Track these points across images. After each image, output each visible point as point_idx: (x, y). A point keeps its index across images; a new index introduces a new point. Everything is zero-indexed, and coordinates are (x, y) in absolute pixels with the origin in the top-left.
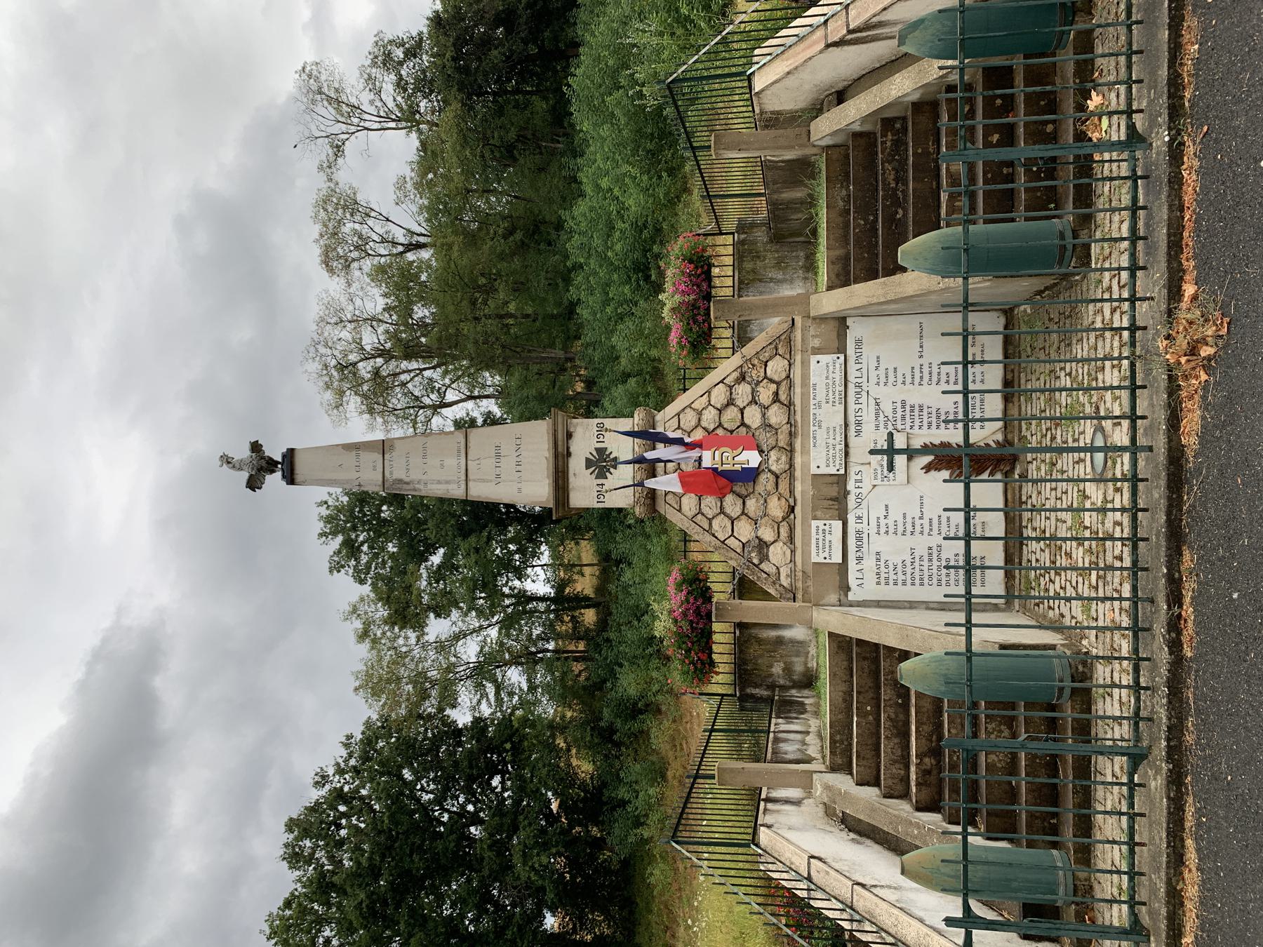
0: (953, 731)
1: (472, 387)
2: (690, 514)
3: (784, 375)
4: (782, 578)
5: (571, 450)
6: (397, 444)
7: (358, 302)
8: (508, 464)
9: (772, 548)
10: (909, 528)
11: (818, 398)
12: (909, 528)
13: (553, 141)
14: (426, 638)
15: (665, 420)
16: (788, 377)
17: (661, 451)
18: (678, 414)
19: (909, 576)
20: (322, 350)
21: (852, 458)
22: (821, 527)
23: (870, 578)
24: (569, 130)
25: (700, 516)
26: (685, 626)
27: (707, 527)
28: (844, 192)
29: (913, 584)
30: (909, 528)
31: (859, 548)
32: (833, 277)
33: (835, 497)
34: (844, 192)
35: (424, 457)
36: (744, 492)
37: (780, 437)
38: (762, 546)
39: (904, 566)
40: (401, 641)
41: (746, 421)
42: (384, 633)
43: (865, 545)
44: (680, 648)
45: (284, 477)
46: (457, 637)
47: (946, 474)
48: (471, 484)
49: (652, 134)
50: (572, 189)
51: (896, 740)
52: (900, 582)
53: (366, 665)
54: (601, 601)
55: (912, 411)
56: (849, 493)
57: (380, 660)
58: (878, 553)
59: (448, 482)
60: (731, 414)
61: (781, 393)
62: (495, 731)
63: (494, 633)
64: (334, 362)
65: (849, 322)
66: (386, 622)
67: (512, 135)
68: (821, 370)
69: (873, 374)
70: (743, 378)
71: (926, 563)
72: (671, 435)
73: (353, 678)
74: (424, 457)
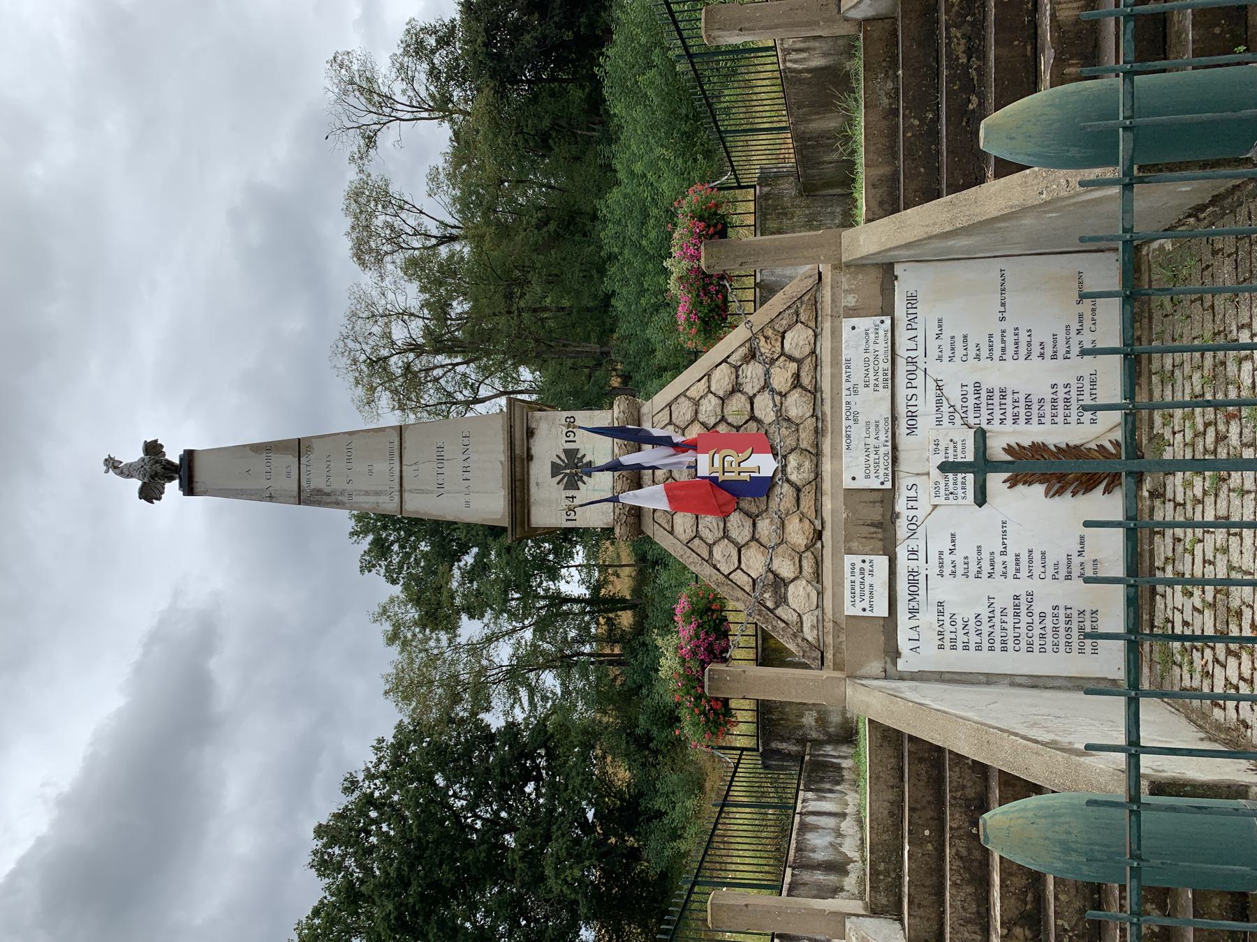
0: (1063, 897)
1: (504, 380)
3: (807, 350)
4: (806, 628)
5: (533, 452)
6: (316, 444)
7: (390, 296)
8: (453, 469)
9: (791, 588)
11: (853, 380)
13: (589, 129)
14: (458, 640)
16: (813, 352)
17: (647, 455)
18: (670, 405)
20: (351, 344)
21: (903, 466)
22: (859, 565)
23: (929, 640)
24: (604, 118)
25: (697, 541)
27: (706, 556)
28: (890, 85)
29: (991, 649)
30: (986, 568)
31: (913, 595)
32: (874, 204)
33: (878, 521)
34: (890, 85)
35: (349, 460)
36: (754, 510)
37: (803, 435)
38: (779, 584)
40: (432, 643)
41: (757, 413)
42: (414, 635)
43: (922, 592)
44: (688, 693)
45: (181, 486)
46: (489, 639)
48: (406, 495)
49: (687, 116)
50: (607, 176)
51: (970, 890)
52: (972, 646)
53: (396, 667)
54: (637, 604)
55: (990, 398)
56: (898, 516)
57: (412, 662)
58: (940, 604)
59: (377, 493)
60: (738, 404)
61: (803, 374)
62: (531, 736)
63: (528, 635)
64: (363, 357)
65: (898, 270)
66: (415, 624)
67: (546, 123)
68: (859, 338)
69: (933, 345)
70: (754, 357)
71: (1010, 619)
72: (657, 432)
73: (382, 681)
74: (349, 460)
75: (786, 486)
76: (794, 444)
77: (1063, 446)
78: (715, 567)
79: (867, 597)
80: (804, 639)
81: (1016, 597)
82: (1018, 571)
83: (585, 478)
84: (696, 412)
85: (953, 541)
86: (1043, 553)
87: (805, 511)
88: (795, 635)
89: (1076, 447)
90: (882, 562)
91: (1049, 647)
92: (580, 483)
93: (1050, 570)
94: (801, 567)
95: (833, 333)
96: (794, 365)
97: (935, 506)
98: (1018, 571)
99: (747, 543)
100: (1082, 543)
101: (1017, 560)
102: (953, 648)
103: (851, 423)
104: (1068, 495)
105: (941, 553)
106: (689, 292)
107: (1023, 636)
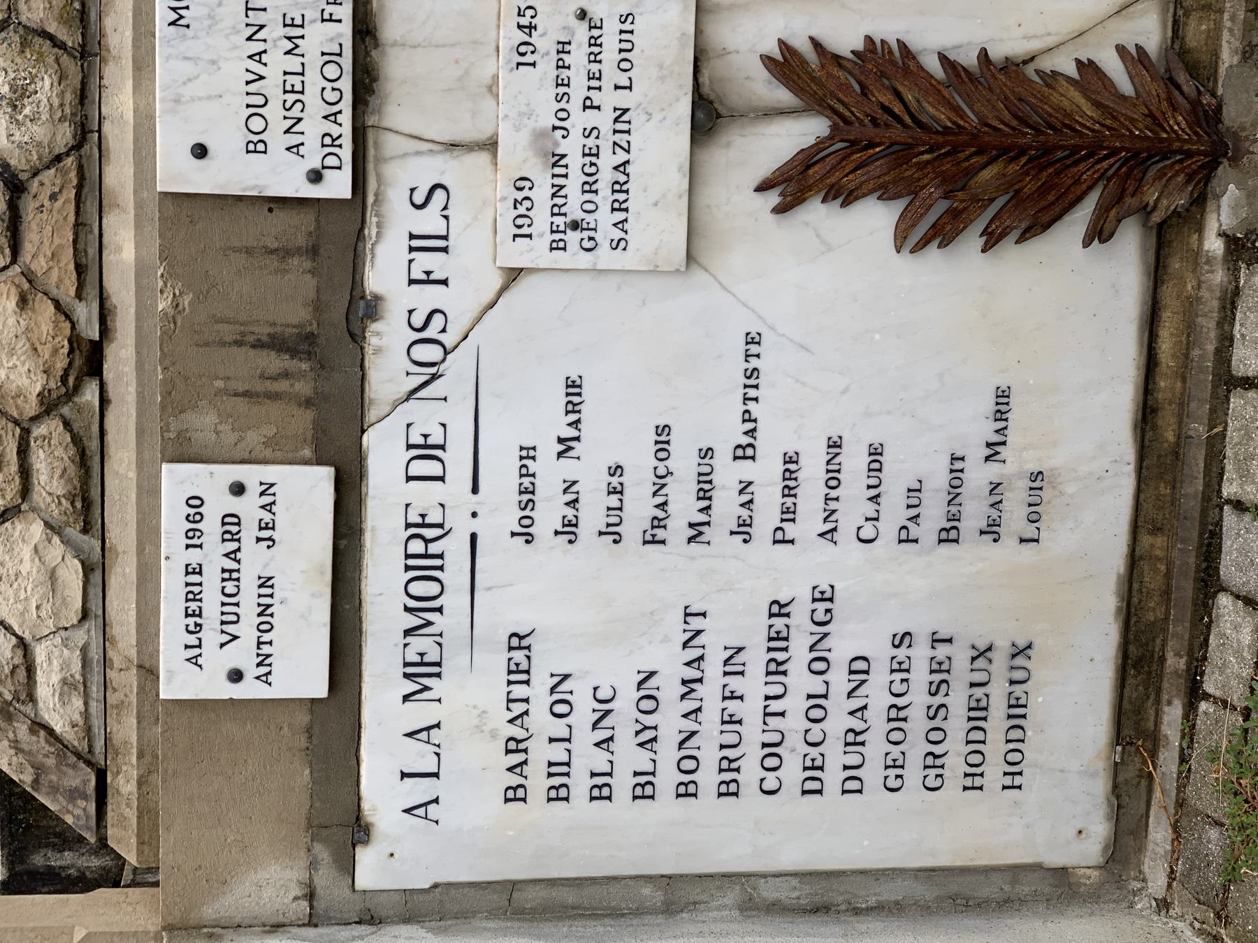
4: (46, 688)
10: (680, 506)
12: (684, 506)
19: (668, 752)
21: (400, 111)
22: (218, 504)
23: (475, 765)
29: (686, 791)
30: (684, 506)
31: (422, 611)
33: (293, 326)
39: (649, 700)
43: (454, 601)
47: (875, 219)
52: (623, 783)
56: (372, 308)
58: (518, 641)
71: (754, 685)
77: (969, 59)
79: (247, 629)
80: (39, 726)
81: (779, 609)
82: (789, 514)
85: (572, 408)
86: (876, 453)
87: (39, 266)
89: (1013, 67)
90: (307, 490)
91: (873, 774)
93: (894, 512)
94: (25, 472)
97: (513, 275)
98: (789, 514)
100: (1000, 415)
101: (789, 475)
102: (559, 795)
104: (972, 240)
105: (528, 453)
107: (795, 741)
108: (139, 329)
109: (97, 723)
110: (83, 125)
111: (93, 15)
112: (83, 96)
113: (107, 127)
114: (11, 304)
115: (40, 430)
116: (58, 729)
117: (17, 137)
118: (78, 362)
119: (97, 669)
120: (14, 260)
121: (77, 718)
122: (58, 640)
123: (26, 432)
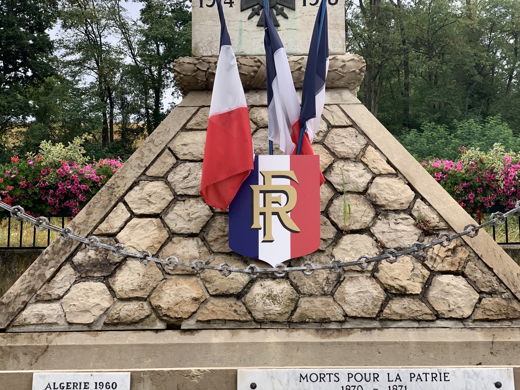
2: (177, 145)
3: (441, 308)
9: (100, 286)
15: (342, 108)
16: (438, 316)
18: (354, 125)
25: (172, 160)
26: (50, 179)
27: (151, 172)
36: (212, 235)
37: (318, 302)
38: (106, 269)
41: (347, 239)
46: (123, 26)
60: (361, 213)
61: (406, 301)
62: (42, 63)
63: (128, 61)
75: (244, 279)
76: (305, 290)
78: (136, 183)
80: (26, 304)
83: (256, 19)
84: (345, 159)
87: (209, 306)
88: (32, 291)
92: (249, 12)
94: (129, 299)
95: (469, 345)
96: (417, 289)
99: (165, 225)
103: (344, 382)
106: (467, 171)
108: (186, 344)
109: (25, 329)
110: (263, 322)
111: (304, 326)
112: (274, 322)
113: (262, 331)
114: (195, 295)
115: (146, 305)
116: (24, 313)
117: (257, 297)
118: (172, 321)
119: (48, 328)
120: (211, 295)
121: (28, 321)
122: (61, 313)
123: (145, 300)
